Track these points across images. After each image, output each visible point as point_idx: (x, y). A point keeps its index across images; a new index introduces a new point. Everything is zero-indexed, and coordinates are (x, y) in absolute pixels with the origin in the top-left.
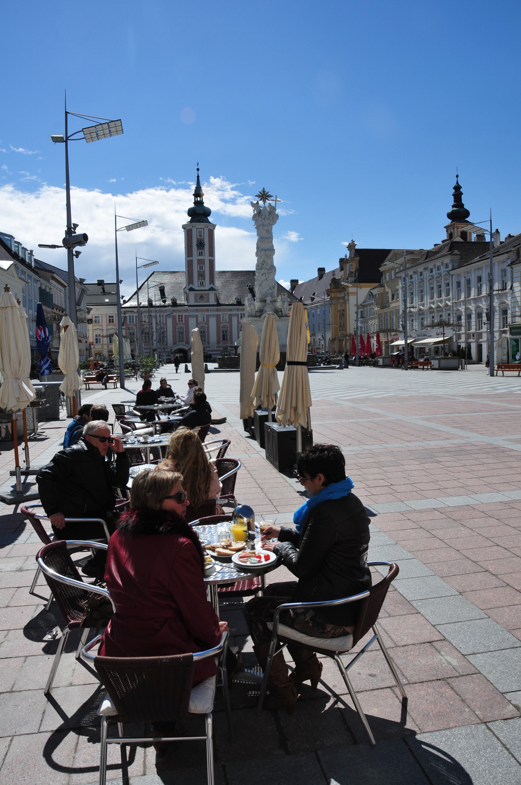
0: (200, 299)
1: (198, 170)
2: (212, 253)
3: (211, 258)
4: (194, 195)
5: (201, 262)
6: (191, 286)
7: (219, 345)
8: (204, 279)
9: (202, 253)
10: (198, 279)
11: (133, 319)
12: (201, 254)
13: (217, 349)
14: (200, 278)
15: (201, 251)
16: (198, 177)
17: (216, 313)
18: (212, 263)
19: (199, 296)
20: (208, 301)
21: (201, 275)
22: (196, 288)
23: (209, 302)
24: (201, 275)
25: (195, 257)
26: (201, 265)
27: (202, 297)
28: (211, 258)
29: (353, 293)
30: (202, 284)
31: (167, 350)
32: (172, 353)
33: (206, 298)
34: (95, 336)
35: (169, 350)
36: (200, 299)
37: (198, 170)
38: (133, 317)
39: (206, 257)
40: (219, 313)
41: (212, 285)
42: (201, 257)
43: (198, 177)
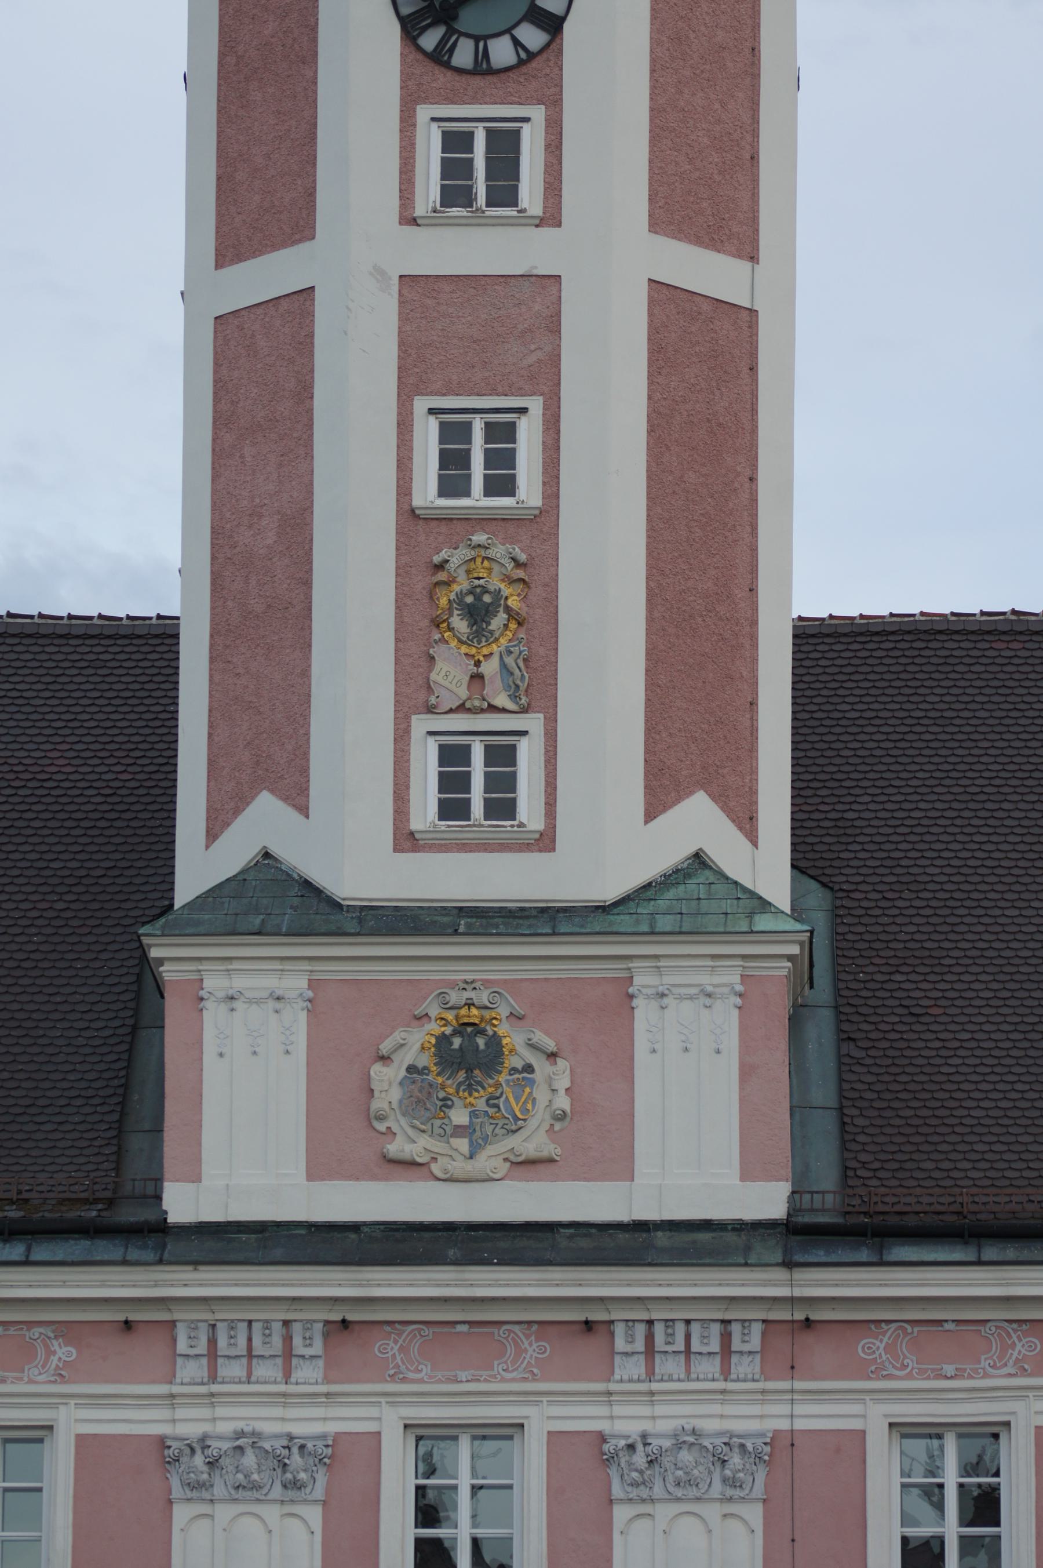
0: (424, 1100)
2: (713, 166)
3: (707, 272)
5: (479, 348)
6: (265, 825)
8: (536, 686)
9: (505, 146)
10: (414, 695)
12: (482, 177)
14: (450, 674)
15: (480, 112)
17: (752, 1410)
19: (414, 1044)
20: (603, 1139)
21: (477, 600)
22: (361, 868)
23: (619, 1164)
24: (477, 600)
25: (369, 238)
27: (469, 1055)
28: (707, 272)
30: (478, 789)
33: (554, 1087)
36: (424, 1100)
39: (605, 253)
40: (817, 1409)
41: (697, 823)
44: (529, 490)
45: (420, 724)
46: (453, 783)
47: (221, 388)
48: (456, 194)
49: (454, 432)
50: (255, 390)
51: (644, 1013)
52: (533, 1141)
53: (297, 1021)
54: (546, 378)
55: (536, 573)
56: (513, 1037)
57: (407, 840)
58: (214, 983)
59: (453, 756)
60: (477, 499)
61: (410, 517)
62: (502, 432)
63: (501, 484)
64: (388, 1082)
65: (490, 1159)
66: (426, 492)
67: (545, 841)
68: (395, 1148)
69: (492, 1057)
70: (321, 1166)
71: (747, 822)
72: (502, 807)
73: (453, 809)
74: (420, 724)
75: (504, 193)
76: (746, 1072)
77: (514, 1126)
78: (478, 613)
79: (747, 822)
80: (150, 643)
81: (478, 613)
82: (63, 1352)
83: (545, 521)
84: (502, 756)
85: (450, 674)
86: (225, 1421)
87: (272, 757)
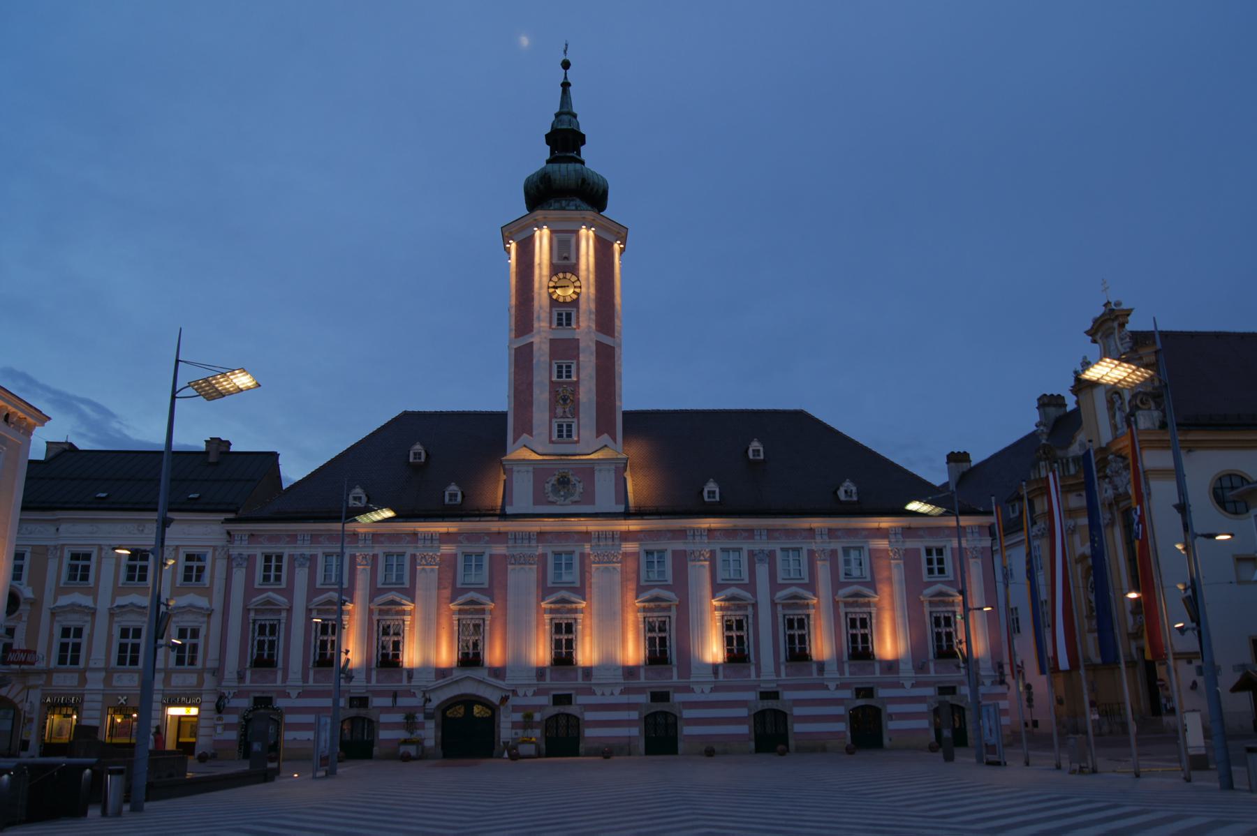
0: (555, 490)
1: (566, 65)
4: (550, 139)
7: (633, 683)
8: (575, 413)
9: (569, 316)
10: (553, 415)
11: (279, 568)
13: (624, 699)
16: (566, 85)
18: (606, 358)
19: (553, 480)
20: (589, 497)
21: (564, 397)
24: (564, 397)
26: (564, 362)
27: (564, 482)
28: (606, 340)
29: (1162, 473)
31: (402, 702)
32: (428, 716)
33: (580, 488)
34: (117, 632)
35: (416, 701)
36: (555, 490)
37: (566, 65)
38: (279, 558)
42: (564, 334)
43: (566, 85)
44: (574, 379)
45: (554, 420)
46: (560, 431)
47: (516, 361)
48: (560, 324)
49: (560, 367)
50: (523, 359)
51: (597, 474)
52: (576, 498)
53: (531, 475)
54: (577, 357)
55: (575, 392)
56: (572, 478)
57: (551, 442)
58: (515, 468)
59: (560, 426)
60: (564, 379)
61: (551, 382)
62: (569, 367)
63: (569, 377)
64: (548, 487)
65: (568, 501)
66: (555, 378)
67: (578, 442)
68: (552, 498)
69: (568, 482)
70: (536, 503)
71: (614, 439)
72: (569, 436)
73: (560, 436)
74: (554, 420)
75: (569, 324)
76: (616, 484)
77: (572, 495)
78: (565, 400)
79: (614, 439)
80: (503, 415)
81: (565, 400)
82: (487, 538)
83: (577, 383)
84: (569, 426)
85: (559, 411)
86: (517, 552)
87: (525, 426)
